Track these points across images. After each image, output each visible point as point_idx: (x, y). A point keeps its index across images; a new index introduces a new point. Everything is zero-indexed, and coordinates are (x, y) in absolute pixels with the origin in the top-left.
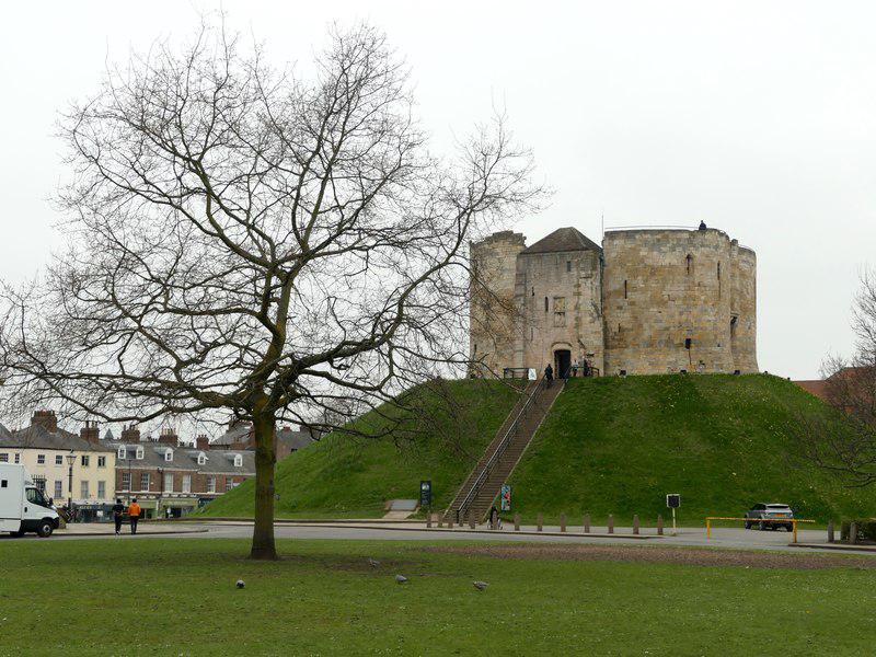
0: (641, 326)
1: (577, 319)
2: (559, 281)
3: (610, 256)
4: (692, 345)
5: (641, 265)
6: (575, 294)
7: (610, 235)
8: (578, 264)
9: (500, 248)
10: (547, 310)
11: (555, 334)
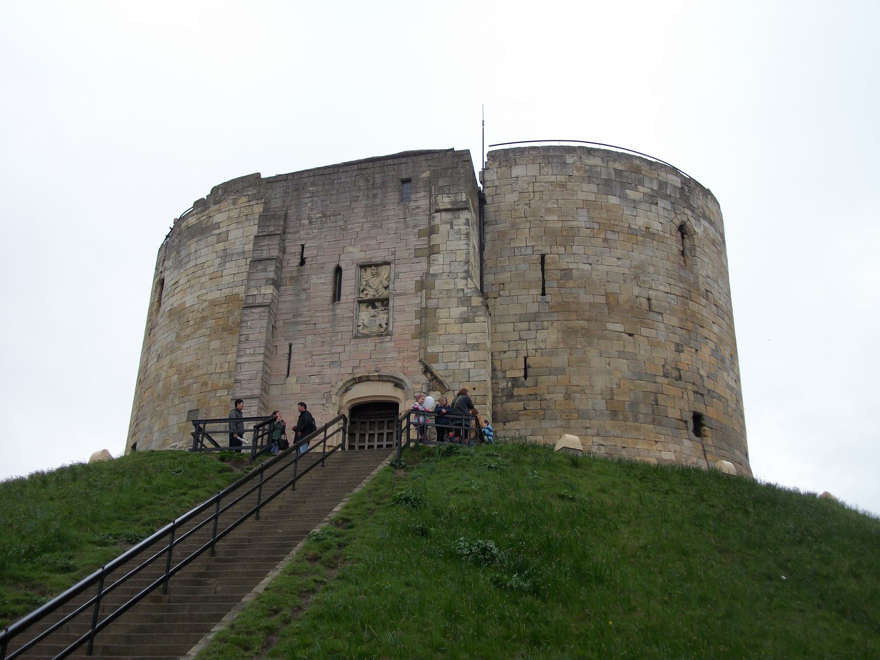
1: (425, 313)
3: (503, 201)
4: (707, 430)
6: (418, 253)
7: (502, 158)
10: (337, 296)
11: (360, 356)
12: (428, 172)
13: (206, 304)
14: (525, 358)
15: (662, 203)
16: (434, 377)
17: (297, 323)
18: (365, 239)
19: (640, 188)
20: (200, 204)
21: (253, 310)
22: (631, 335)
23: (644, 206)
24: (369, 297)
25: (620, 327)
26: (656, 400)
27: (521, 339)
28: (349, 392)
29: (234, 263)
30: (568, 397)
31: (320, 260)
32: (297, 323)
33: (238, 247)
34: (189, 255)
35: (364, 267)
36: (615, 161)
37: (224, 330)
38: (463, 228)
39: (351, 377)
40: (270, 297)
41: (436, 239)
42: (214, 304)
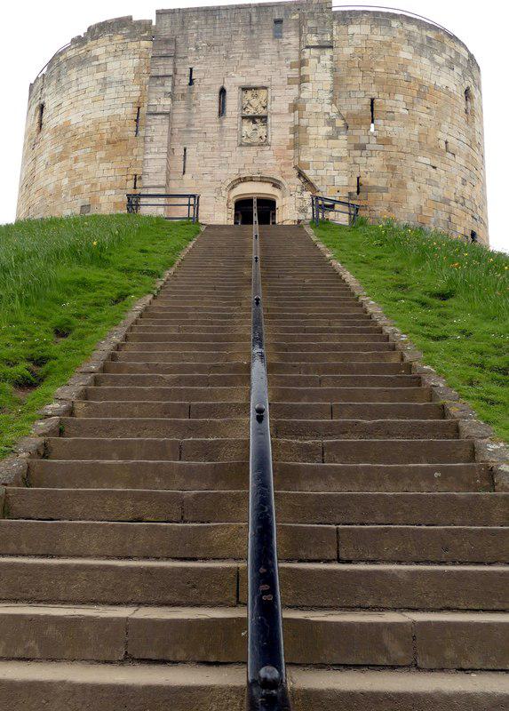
0: (402, 185)
1: (296, 129)
2: (255, 55)
5: (402, 76)
6: (290, 81)
8: (300, 24)
9: (99, 49)
10: (222, 112)
11: (244, 161)
12: (297, 15)
13: (89, 123)
14: (358, 178)
15: (458, 70)
16: (307, 181)
17: (190, 132)
18: (245, 66)
19: (444, 55)
20: (79, 41)
21: (155, 117)
22: (434, 167)
23: (446, 69)
24: (250, 114)
25: (428, 161)
26: (450, 218)
27: (355, 163)
28: (235, 189)
29: (113, 90)
30: (390, 209)
31: (208, 81)
32: (190, 132)
33: (116, 77)
34: (71, 82)
35: (245, 89)
36: (427, 29)
37: (108, 143)
38: (329, 63)
39: (237, 177)
40: (169, 107)
41: (306, 70)
42: (97, 123)
